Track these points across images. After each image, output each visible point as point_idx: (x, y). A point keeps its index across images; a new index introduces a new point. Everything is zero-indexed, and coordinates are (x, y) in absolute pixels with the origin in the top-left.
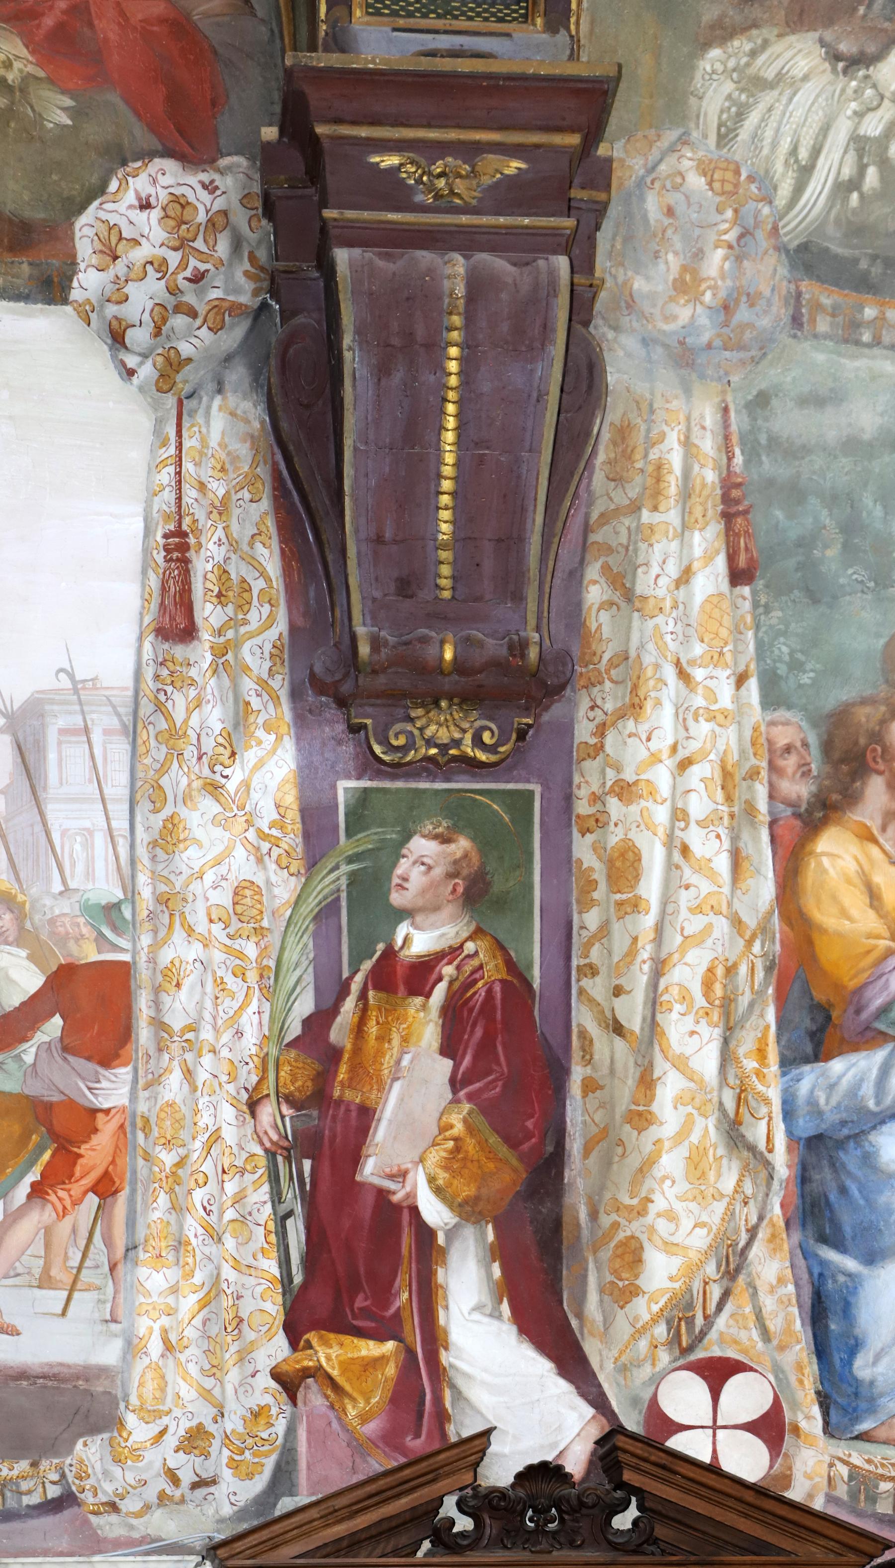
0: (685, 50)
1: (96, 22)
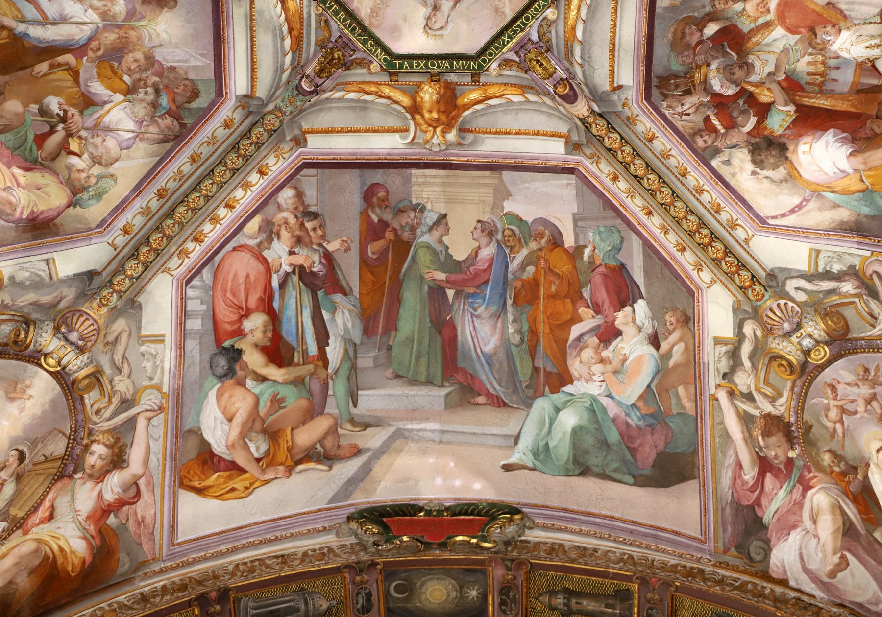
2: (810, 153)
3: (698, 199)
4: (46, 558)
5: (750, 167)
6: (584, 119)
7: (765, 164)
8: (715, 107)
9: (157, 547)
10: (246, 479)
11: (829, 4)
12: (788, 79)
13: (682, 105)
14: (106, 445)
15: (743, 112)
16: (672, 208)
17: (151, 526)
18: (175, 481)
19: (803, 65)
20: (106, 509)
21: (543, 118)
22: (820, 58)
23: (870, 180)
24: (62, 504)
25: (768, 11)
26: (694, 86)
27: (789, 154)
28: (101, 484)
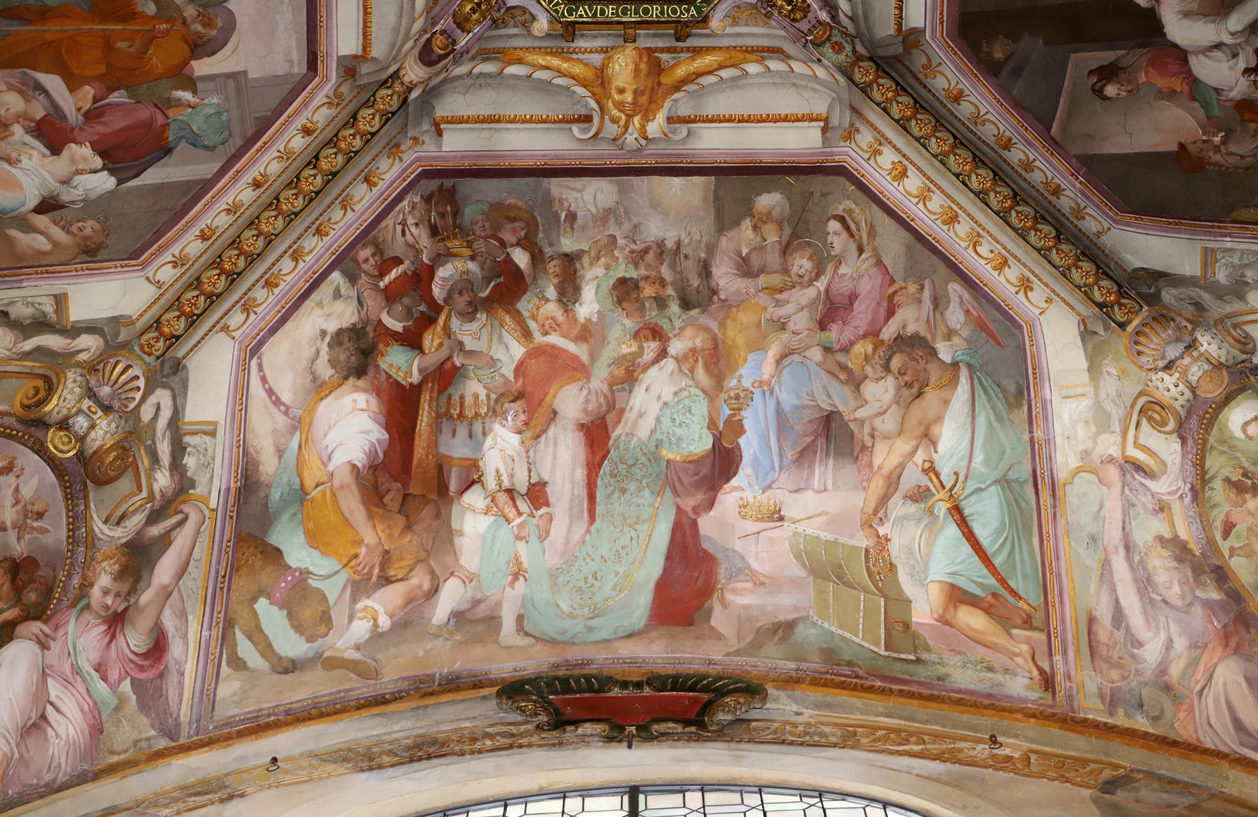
2: (353, 410)
3: (285, 252)
5: (332, 327)
6: (398, 77)
7: (337, 349)
8: (414, 272)
11: (555, 413)
12: (456, 369)
13: (417, 225)
15: (409, 311)
16: (274, 213)
19: (474, 389)
21: (391, 19)
22: (483, 411)
23: (319, 497)
25: (546, 334)
26: (443, 240)
27: (352, 380)
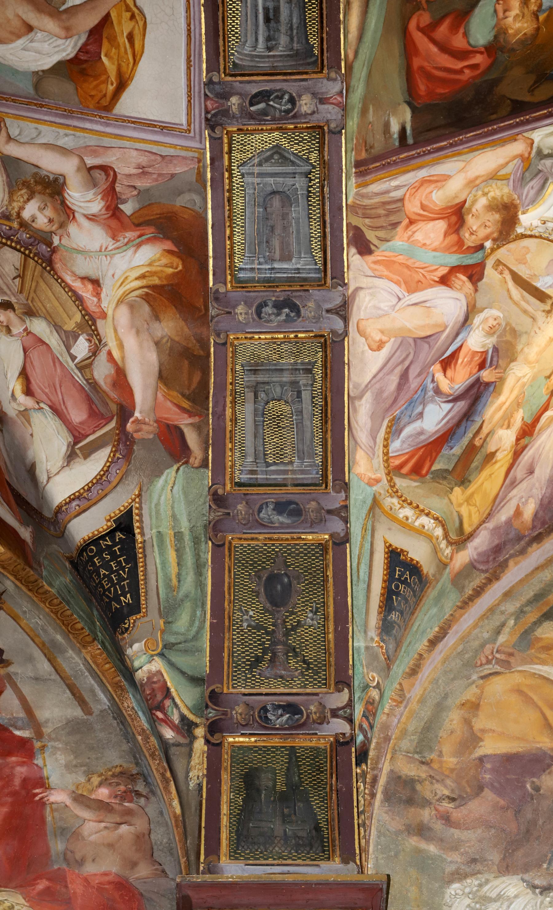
0: (437, 885)
1: (70, 886)
4: (146, 298)
9: (183, 153)
10: (119, 16)
14: (28, 200)
17: (153, 157)
18: (101, 117)
20: (111, 212)
24: (84, 266)
28: (77, 215)
